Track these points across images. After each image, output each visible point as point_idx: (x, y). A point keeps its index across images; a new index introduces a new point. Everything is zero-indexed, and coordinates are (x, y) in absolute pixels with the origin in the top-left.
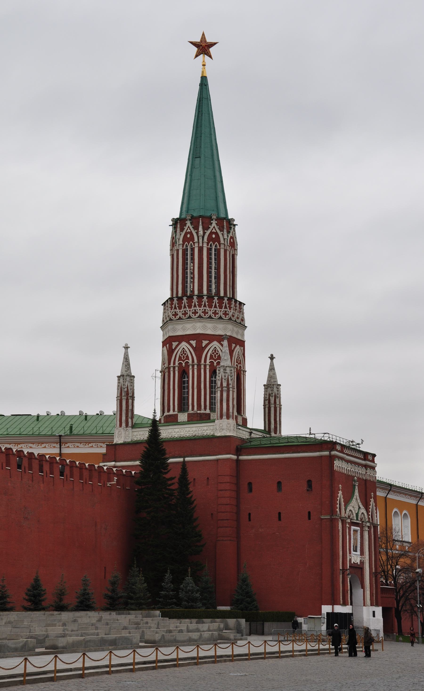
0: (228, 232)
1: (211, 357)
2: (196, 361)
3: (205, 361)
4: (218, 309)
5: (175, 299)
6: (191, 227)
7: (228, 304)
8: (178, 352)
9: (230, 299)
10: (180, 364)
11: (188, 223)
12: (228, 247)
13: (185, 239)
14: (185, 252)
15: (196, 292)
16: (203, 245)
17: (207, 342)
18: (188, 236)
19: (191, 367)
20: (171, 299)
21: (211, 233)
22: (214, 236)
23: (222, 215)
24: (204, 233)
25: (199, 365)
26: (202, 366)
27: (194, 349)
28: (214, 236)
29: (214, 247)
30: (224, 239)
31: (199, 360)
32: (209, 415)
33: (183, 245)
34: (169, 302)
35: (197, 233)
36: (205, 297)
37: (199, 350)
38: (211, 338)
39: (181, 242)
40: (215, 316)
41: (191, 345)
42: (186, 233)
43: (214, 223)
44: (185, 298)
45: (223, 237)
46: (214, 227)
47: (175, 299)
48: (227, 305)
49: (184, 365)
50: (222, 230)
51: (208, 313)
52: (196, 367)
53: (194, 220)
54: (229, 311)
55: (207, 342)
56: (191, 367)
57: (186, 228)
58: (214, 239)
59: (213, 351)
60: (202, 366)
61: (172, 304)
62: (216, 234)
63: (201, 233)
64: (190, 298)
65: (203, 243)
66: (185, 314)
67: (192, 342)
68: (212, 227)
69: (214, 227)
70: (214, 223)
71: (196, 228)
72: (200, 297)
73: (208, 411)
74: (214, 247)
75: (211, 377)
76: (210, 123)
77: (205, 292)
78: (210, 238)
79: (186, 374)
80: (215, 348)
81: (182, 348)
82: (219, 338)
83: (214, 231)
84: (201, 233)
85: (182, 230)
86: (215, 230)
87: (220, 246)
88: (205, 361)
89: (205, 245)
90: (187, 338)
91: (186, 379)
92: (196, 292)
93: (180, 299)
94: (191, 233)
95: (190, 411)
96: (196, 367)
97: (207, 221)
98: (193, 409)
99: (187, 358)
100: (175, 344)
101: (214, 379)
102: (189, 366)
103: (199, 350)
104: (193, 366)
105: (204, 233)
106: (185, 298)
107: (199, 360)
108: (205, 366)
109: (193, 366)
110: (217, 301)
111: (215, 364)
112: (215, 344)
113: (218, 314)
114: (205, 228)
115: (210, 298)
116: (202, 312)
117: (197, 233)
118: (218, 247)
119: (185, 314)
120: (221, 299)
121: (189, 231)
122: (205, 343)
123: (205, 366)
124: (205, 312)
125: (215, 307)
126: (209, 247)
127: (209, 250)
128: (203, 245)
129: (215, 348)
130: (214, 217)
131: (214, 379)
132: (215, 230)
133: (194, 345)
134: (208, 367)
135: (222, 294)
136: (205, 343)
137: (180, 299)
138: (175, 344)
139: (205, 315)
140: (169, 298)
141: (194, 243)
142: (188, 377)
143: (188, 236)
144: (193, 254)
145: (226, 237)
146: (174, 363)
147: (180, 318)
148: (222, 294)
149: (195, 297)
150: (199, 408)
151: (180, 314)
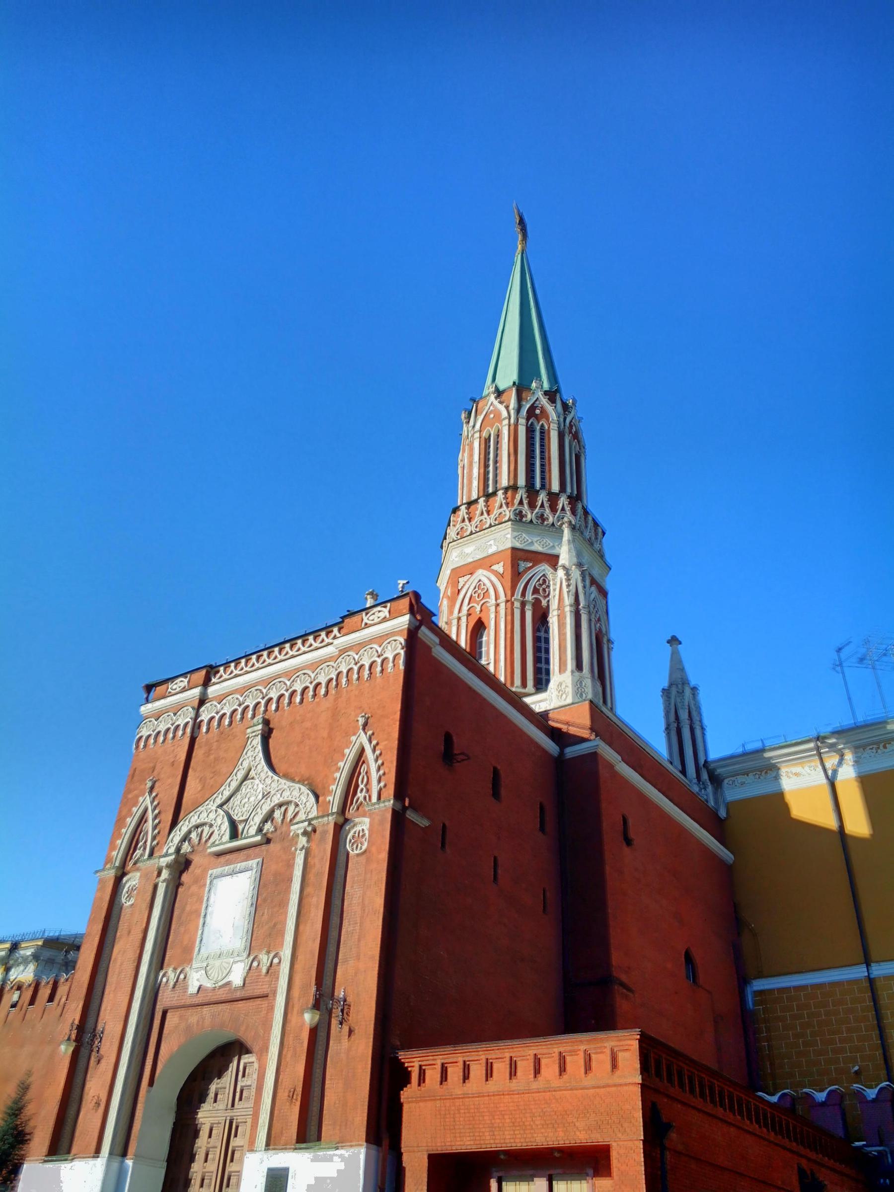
2: (502, 598)
5: (463, 508)
6: (496, 403)
21: (533, 408)
22: (538, 412)
27: (500, 576)
41: (495, 573)
44: (482, 500)
47: (463, 508)
49: (478, 609)
56: (493, 609)
63: (513, 403)
67: (495, 567)
78: (531, 412)
81: (476, 581)
89: (522, 421)
90: (486, 563)
96: (503, 606)
117: (507, 407)
120: (553, 498)
122: (523, 565)
124: (520, 515)
127: (530, 431)
133: (501, 570)
138: (462, 581)
143: (492, 416)
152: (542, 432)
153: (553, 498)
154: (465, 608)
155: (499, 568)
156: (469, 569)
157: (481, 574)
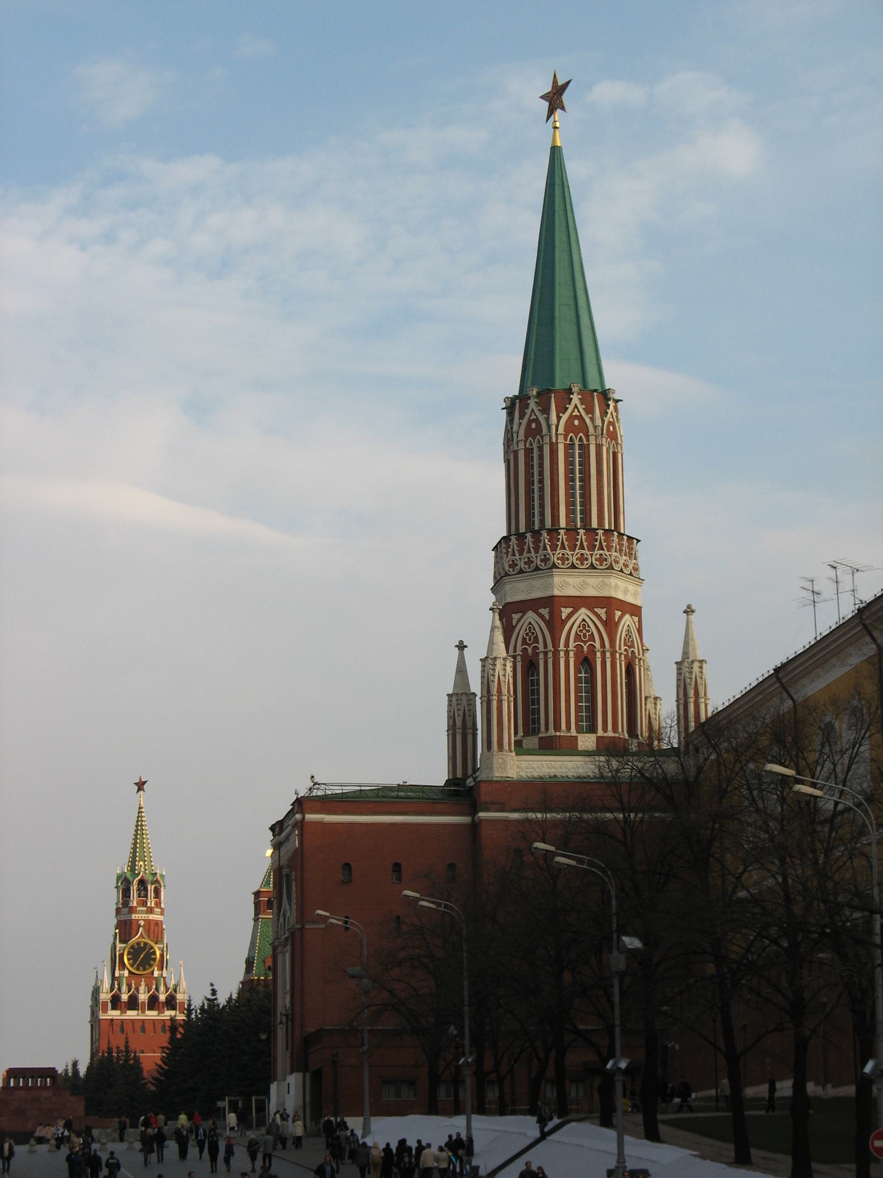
0: (604, 413)
3: (567, 644)
4: (586, 552)
5: (513, 538)
8: (520, 631)
9: (608, 532)
10: (524, 650)
12: (604, 439)
14: (529, 452)
15: (548, 524)
16: (557, 439)
17: (569, 610)
18: (533, 426)
19: (541, 656)
22: (576, 422)
23: (593, 385)
24: (559, 418)
25: (556, 653)
26: (562, 654)
28: (576, 422)
29: (577, 443)
30: (595, 427)
31: (556, 645)
32: (576, 738)
33: (525, 442)
34: (503, 545)
35: (547, 419)
36: (562, 532)
37: (554, 625)
38: (577, 602)
39: (522, 436)
40: (582, 564)
41: (542, 616)
42: (530, 422)
43: (576, 399)
44: (528, 535)
46: (576, 406)
47: (513, 538)
48: (604, 544)
51: (568, 559)
52: (550, 655)
54: (607, 553)
55: (569, 610)
56: (541, 656)
57: (528, 411)
58: (577, 427)
59: (579, 627)
60: (562, 654)
61: (509, 547)
62: (580, 418)
64: (537, 534)
65: (557, 435)
66: (529, 562)
68: (571, 408)
69: (576, 406)
71: (546, 411)
72: (554, 531)
73: (573, 732)
74: (577, 443)
75: (578, 671)
76: (567, 222)
77: (563, 523)
79: (535, 667)
80: (584, 620)
82: (591, 602)
83: (576, 413)
86: (579, 411)
87: (588, 440)
88: (567, 644)
89: (561, 439)
90: (534, 605)
91: (535, 678)
92: (548, 524)
93: (521, 537)
94: (537, 421)
96: (550, 655)
98: (547, 729)
99: (536, 640)
100: (516, 617)
101: (583, 675)
102: (538, 654)
104: (546, 654)
105: (559, 418)
106: (528, 535)
108: (567, 653)
109: (546, 654)
110: (565, 537)
111: (585, 648)
112: (583, 613)
113: (587, 559)
114: (562, 409)
115: (572, 531)
116: (558, 559)
118: (585, 442)
119: (529, 562)
121: (533, 417)
122: (565, 612)
123: (567, 653)
125: (582, 547)
126: (568, 442)
127: (569, 447)
128: (557, 439)
129: (584, 620)
130: (575, 389)
131: (583, 675)
132: (579, 411)
134: (571, 654)
135: (594, 524)
136: (565, 612)
137: (521, 537)
138: (516, 617)
139: (563, 564)
140: (504, 538)
141: (542, 437)
142: (538, 675)
143: (533, 426)
144: (541, 457)
145: (598, 422)
146: (515, 651)
147: (521, 571)
149: (544, 534)
151: (522, 565)
152: (581, 446)
154: (519, 647)
156: (523, 606)
157: (531, 616)
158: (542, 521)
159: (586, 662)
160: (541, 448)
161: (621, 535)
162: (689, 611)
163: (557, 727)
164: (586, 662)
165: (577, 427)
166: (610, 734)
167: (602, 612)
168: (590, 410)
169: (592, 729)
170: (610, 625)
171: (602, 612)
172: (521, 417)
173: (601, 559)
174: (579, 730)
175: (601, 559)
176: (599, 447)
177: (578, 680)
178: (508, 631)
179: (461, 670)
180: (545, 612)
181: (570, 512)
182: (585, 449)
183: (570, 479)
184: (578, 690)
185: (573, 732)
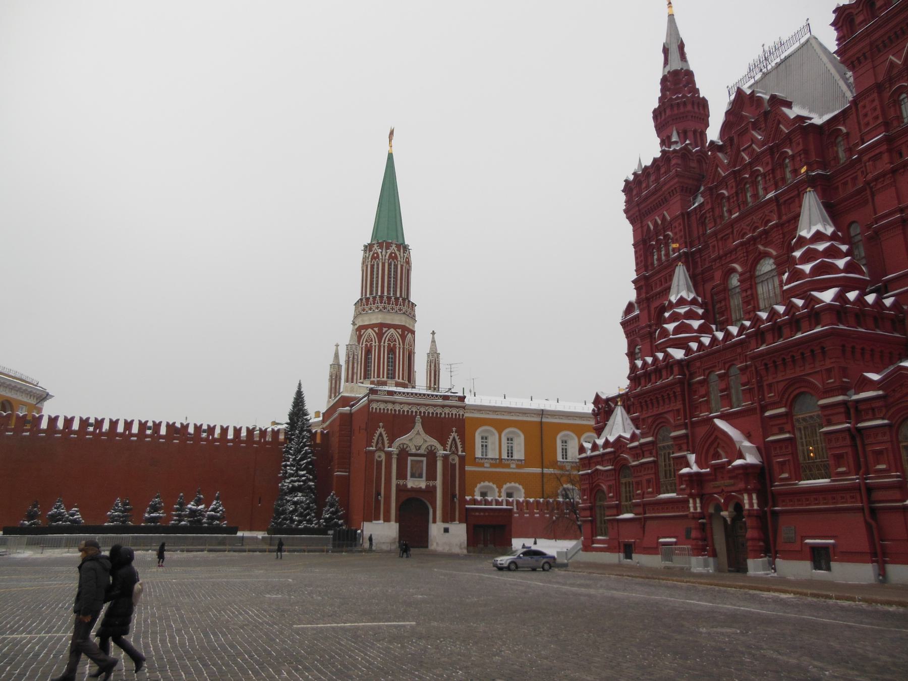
1: (389, 340)
7: (404, 303)
11: (375, 246)
13: (373, 258)
14: (372, 267)
20: (361, 299)
38: (389, 326)
43: (394, 246)
45: (400, 255)
50: (399, 250)
53: (380, 245)
58: (393, 257)
63: (384, 253)
64: (374, 298)
70: (394, 246)
72: (381, 297)
73: (385, 379)
75: (388, 354)
77: (386, 294)
82: (396, 327)
84: (384, 253)
85: (370, 251)
90: (372, 326)
93: (367, 299)
94: (377, 253)
95: (372, 379)
97: (388, 246)
103: (380, 335)
107: (380, 342)
112: (392, 330)
114: (387, 248)
122: (385, 330)
124: (385, 308)
127: (390, 265)
136: (385, 330)
138: (363, 331)
144: (378, 268)
148: (398, 295)
150: (378, 376)
153: (397, 299)
155: (376, 329)
156: (366, 327)
157: (370, 330)
158: (377, 293)
159: (392, 350)
160: (378, 265)
161: (409, 301)
162: (433, 333)
163: (378, 376)
164: (392, 350)
165: (393, 257)
166: (400, 380)
167: (400, 331)
168: (399, 250)
169: (394, 378)
170: (403, 337)
171: (400, 331)
172: (370, 251)
173: (400, 310)
174: (388, 378)
175: (400, 310)
176: (402, 266)
177: (388, 358)
178: (359, 337)
179: (337, 356)
180: (376, 329)
181: (389, 291)
182: (396, 266)
183: (389, 277)
184: (388, 362)
185: (385, 379)
